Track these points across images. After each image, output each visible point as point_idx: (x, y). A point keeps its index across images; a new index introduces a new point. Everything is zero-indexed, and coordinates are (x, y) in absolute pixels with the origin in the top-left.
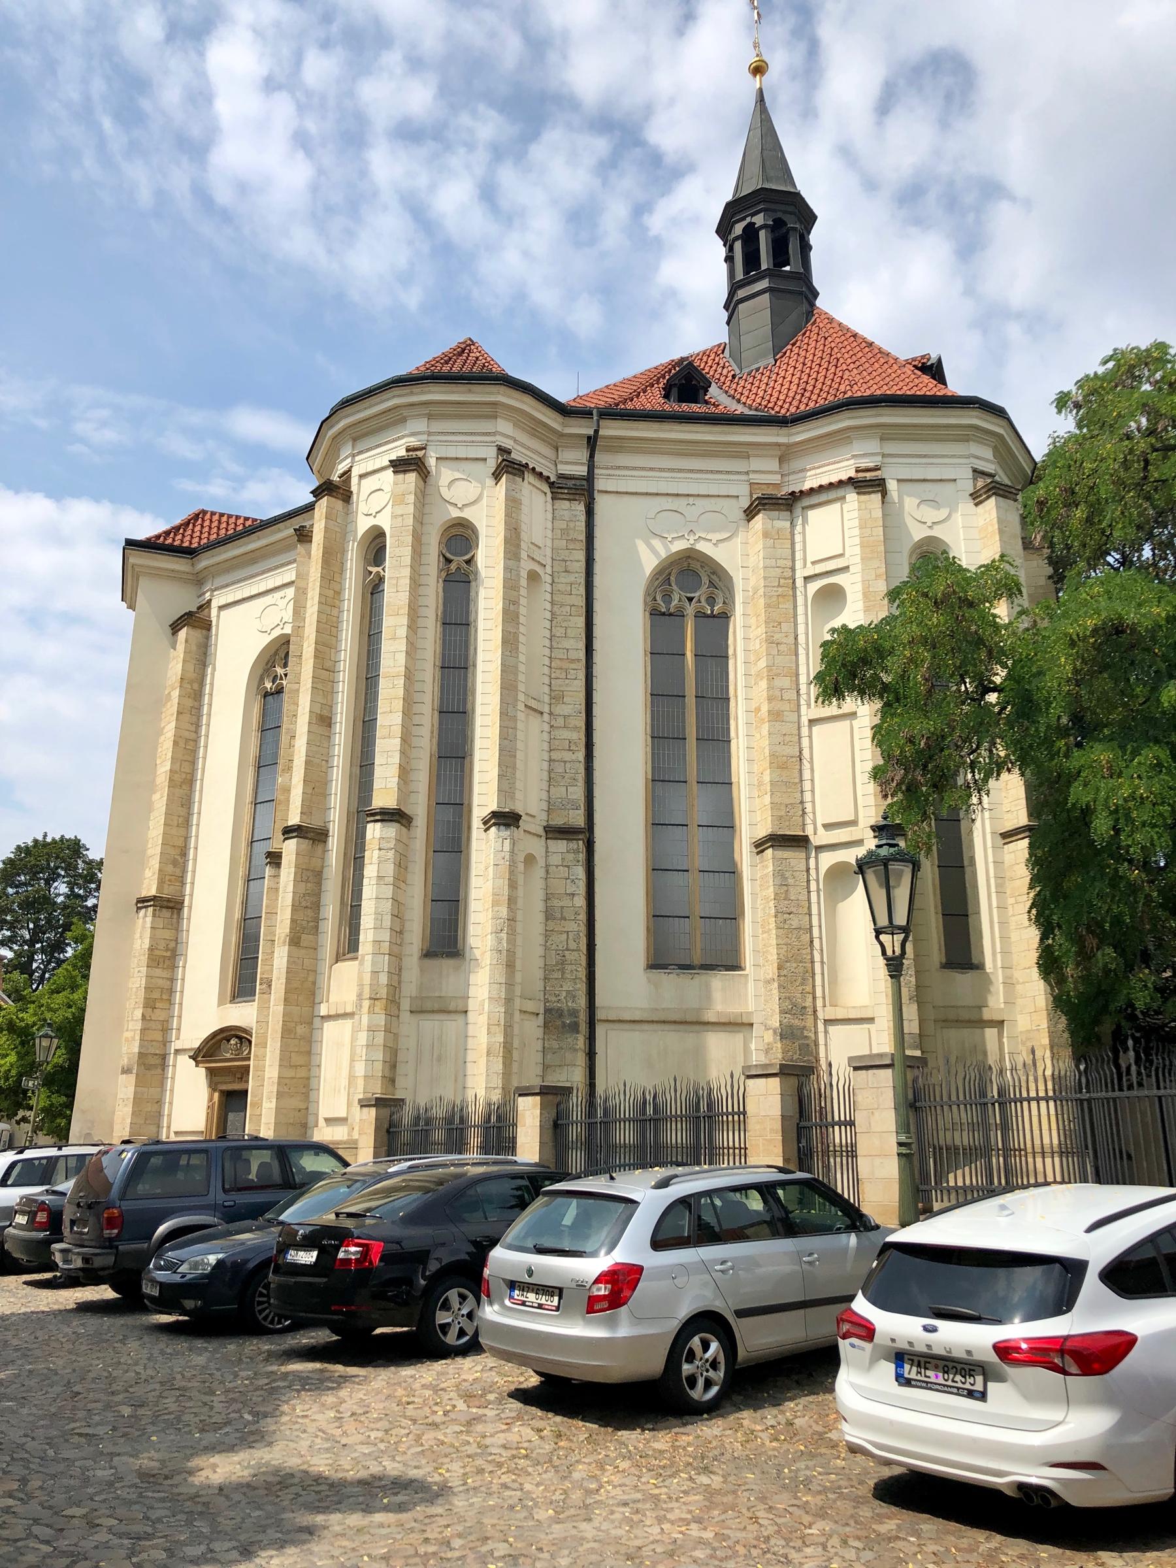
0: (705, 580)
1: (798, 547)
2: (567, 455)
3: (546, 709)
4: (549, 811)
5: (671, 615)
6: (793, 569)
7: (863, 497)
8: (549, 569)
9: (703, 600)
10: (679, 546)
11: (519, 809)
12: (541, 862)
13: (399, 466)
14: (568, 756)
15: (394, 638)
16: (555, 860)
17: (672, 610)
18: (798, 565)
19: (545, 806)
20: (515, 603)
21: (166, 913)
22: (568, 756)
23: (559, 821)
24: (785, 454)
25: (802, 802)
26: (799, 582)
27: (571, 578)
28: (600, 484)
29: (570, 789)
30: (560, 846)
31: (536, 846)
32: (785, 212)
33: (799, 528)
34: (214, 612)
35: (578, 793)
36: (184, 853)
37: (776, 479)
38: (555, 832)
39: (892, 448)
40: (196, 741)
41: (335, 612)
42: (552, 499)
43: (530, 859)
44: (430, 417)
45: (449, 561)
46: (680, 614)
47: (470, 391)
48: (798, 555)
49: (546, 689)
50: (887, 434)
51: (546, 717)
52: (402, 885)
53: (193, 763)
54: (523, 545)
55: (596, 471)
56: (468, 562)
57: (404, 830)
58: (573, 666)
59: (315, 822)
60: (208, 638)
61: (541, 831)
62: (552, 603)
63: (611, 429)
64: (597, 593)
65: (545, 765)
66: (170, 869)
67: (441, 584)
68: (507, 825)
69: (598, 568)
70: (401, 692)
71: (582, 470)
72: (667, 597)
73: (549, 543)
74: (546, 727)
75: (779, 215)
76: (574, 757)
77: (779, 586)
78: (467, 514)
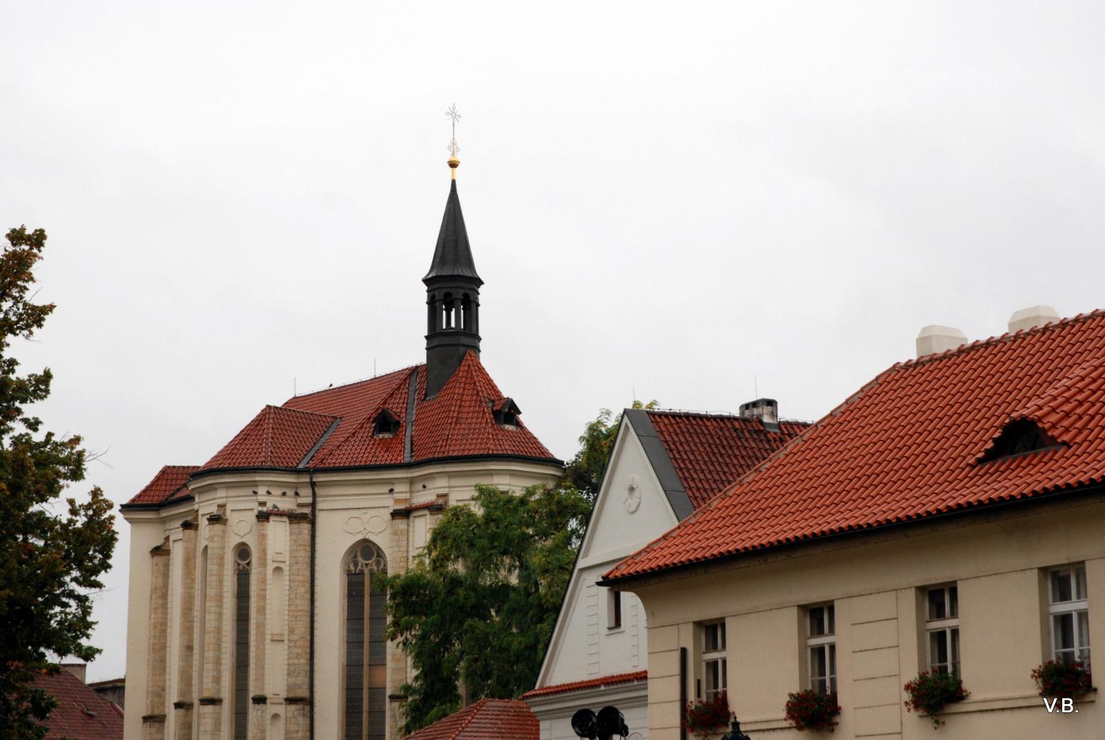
0: (376, 554)
1: (411, 539)
2: (302, 492)
3: (286, 638)
4: (288, 690)
5: (358, 574)
6: (407, 551)
7: (433, 517)
8: (287, 563)
9: (374, 565)
10: (359, 537)
11: (268, 693)
12: (283, 716)
13: (215, 519)
14: (296, 661)
15: (210, 613)
16: (290, 715)
17: (357, 572)
18: (411, 549)
19: (285, 688)
20: (264, 590)
21: (157, 725)
22: (296, 661)
23: (292, 695)
24: (412, 481)
25: (406, 678)
26: (411, 559)
27: (299, 567)
28: (319, 506)
29: (298, 678)
30: (293, 707)
31: (281, 710)
32: (451, 288)
33: (411, 529)
34: (171, 543)
35: (303, 680)
36: (164, 689)
37: (408, 496)
38: (290, 701)
39: (454, 482)
40: (166, 624)
41: (192, 591)
42: (290, 523)
43: (276, 716)
44: (227, 488)
45: (239, 564)
46: (362, 573)
47: (242, 476)
48: (411, 544)
49: (286, 627)
50: (451, 475)
51: (286, 642)
52: (218, 733)
53: (165, 637)
54: (269, 557)
55: (317, 499)
56: (248, 564)
57: (217, 707)
58: (300, 614)
59: (186, 700)
60: (169, 560)
61: (283, 701)
62: (290, 581)
63: (320, 478)
64: (317, 568)
65: (286, 667)
66: (157, 699)
67: (236, 576)
68: (259, 703)
69: (318, 554)
70: (213, 640)
71: (309, 500)
72: (356, 564)
73: (288, 548)
74: (286, 647)
75: (449, 290)
76: (299, 662)
77: (400, 562)
78: (244, 540)
